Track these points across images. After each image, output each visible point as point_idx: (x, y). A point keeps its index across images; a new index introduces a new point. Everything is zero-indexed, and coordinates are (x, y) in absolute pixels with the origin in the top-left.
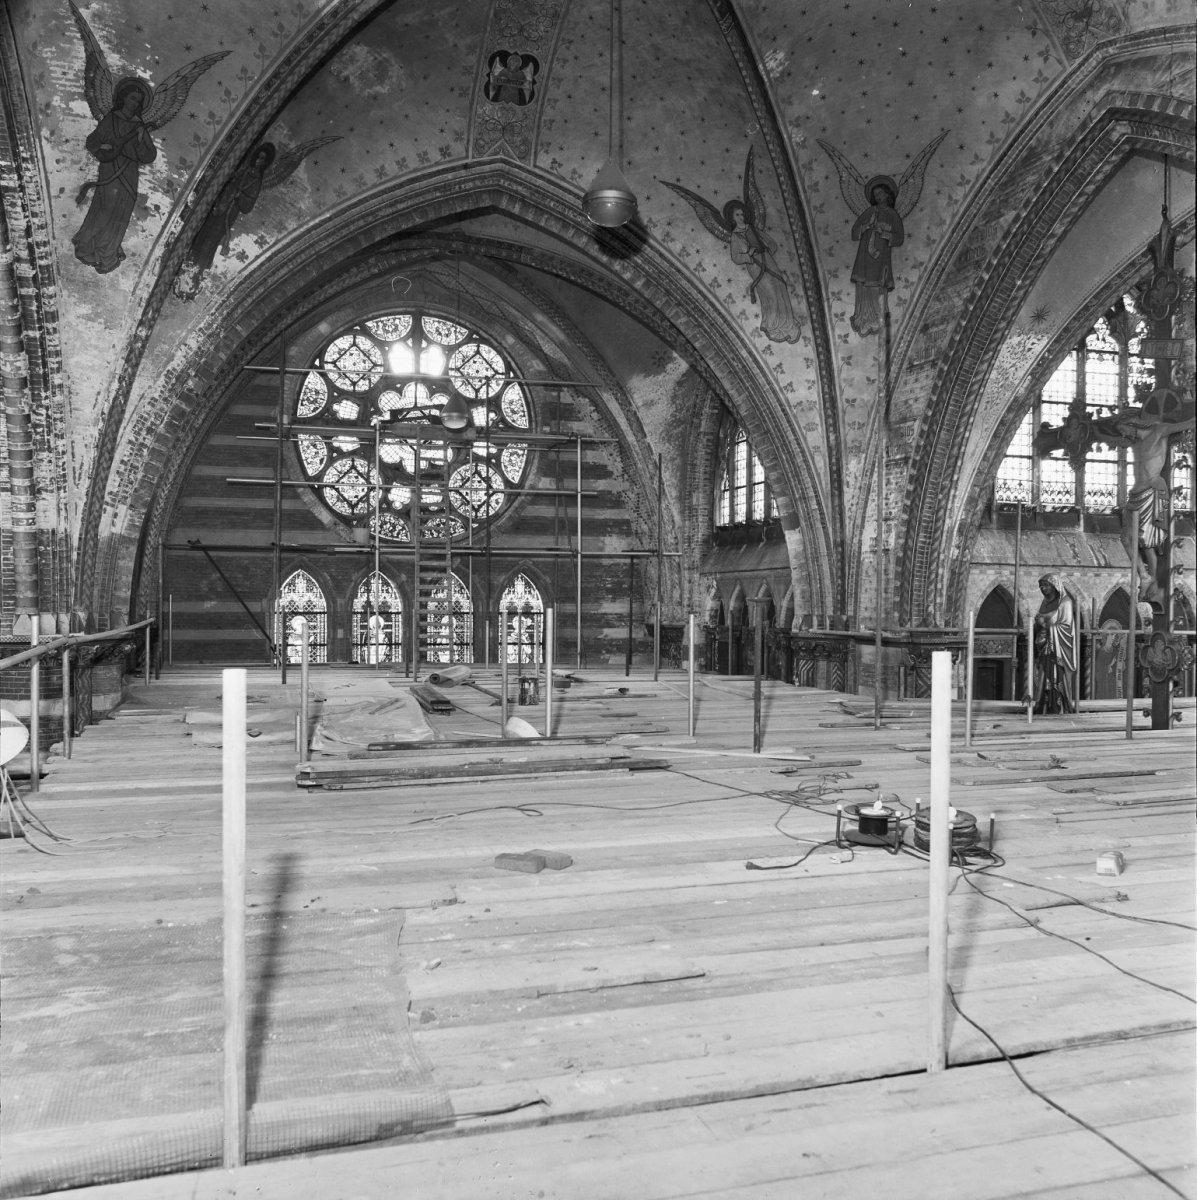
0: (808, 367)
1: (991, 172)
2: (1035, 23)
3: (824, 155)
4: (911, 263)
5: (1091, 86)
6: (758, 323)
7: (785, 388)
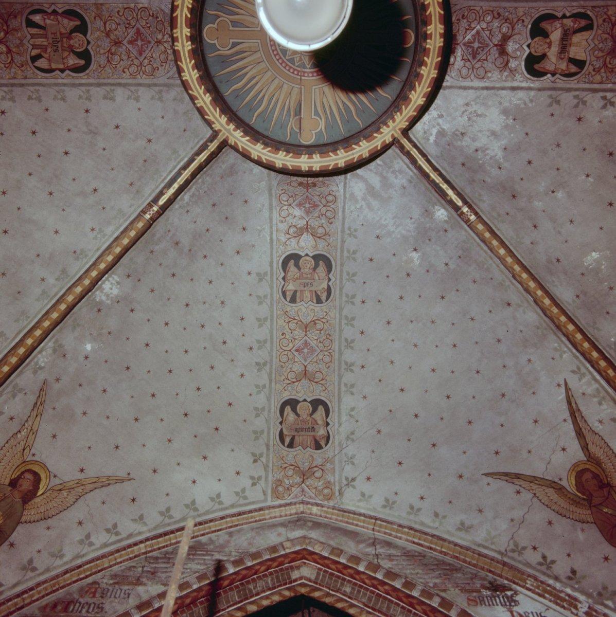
1: (147, 540)
2: (261, 455)
3: (32, 399)
5: (283, 525)
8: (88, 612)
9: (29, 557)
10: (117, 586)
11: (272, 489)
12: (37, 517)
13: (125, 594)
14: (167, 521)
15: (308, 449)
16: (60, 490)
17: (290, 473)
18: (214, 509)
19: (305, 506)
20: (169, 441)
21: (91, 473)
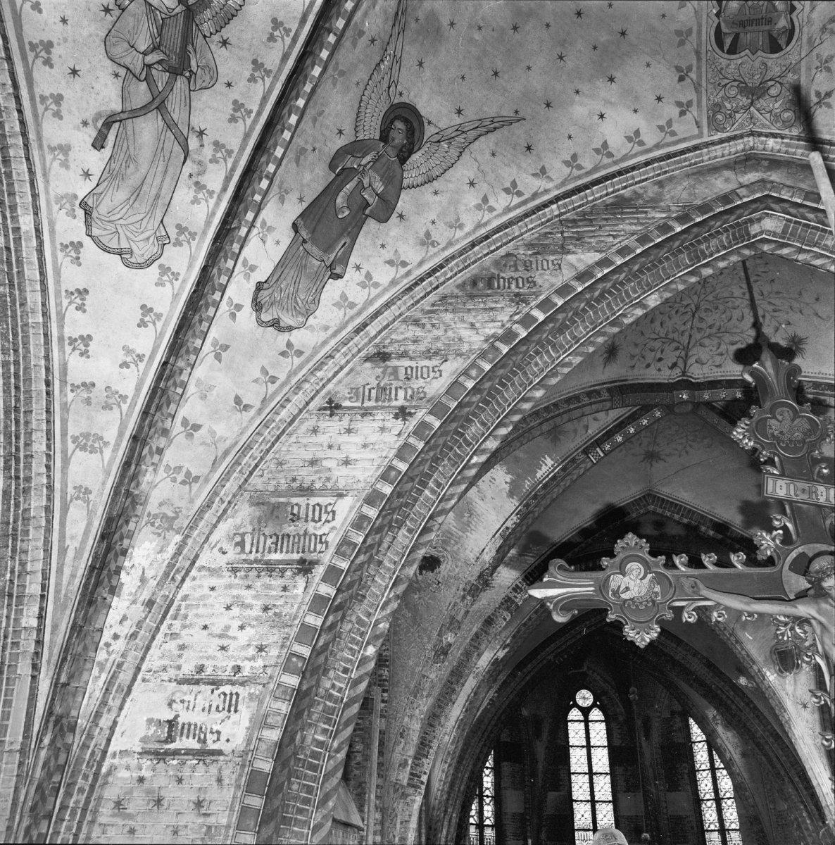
0: (142, 324)
1: (557, 199)
2: (689, 69)
4: (387, 254)
5: (728, 166)
6: (83, 189)
7: (72, 341)
8: (517, 286)
9: (424, 230)
10: (539, 257)
11: (708, 118)
12: (420, 179)
13: (553, 264)
14: (576, 172)
15: (760, 53)
16: (439, 141)
17: (733, 92)
18: (633, 152)
19: (756, 139)
20: (561, 58)
21: (471, 114)
